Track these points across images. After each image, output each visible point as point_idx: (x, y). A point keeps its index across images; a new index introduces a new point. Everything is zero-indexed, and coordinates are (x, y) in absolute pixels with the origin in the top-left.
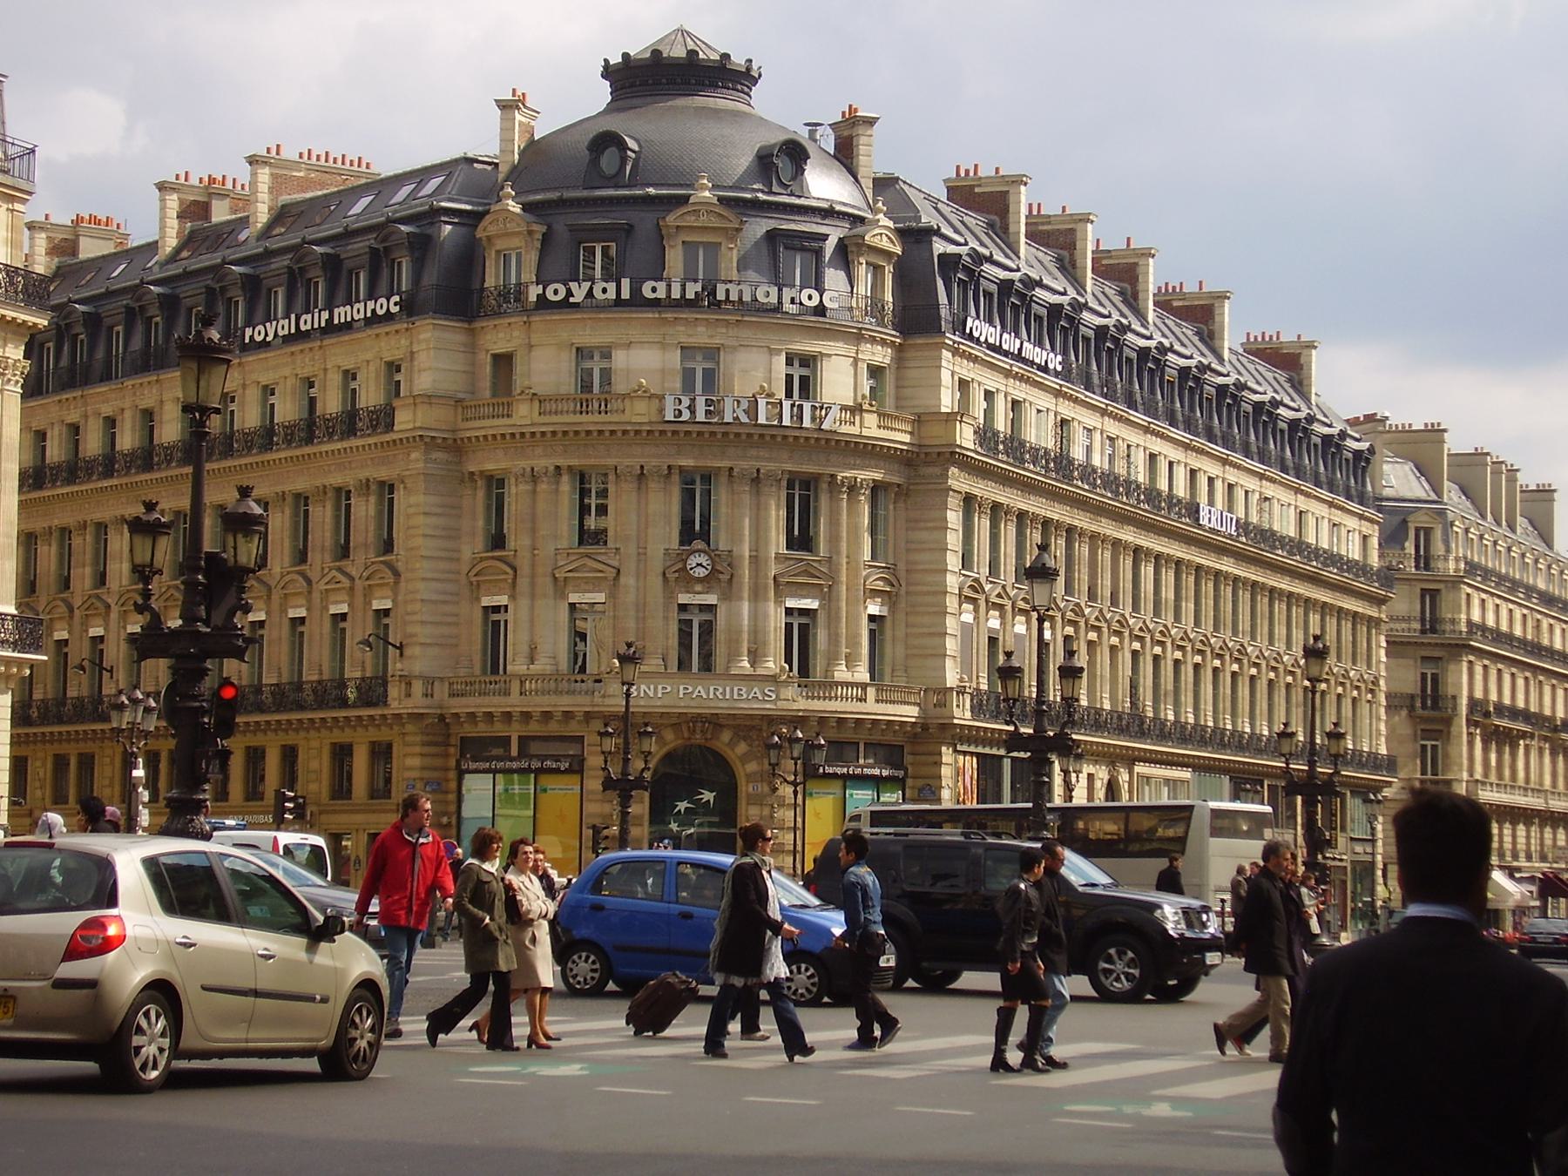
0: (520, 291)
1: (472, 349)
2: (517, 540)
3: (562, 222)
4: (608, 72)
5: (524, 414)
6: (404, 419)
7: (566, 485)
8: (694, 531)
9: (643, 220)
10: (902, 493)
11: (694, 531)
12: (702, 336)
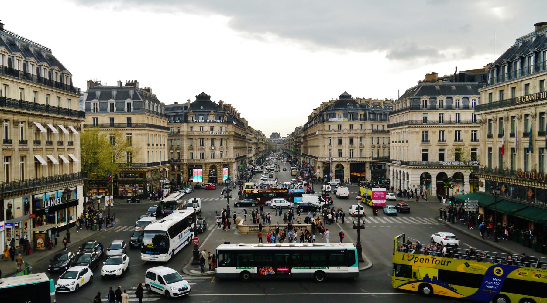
0: (193, 120)
1: (188, 126)
2: (194, 146)
3: (197, 114)
4: (197, 97)
5: (195, 133)
6: (181, 133)
7: (199, 140)
8: (212, 145)
9: (206, 114)
10: (228, 139)
11: (212, 145)
12: (212, 125)
